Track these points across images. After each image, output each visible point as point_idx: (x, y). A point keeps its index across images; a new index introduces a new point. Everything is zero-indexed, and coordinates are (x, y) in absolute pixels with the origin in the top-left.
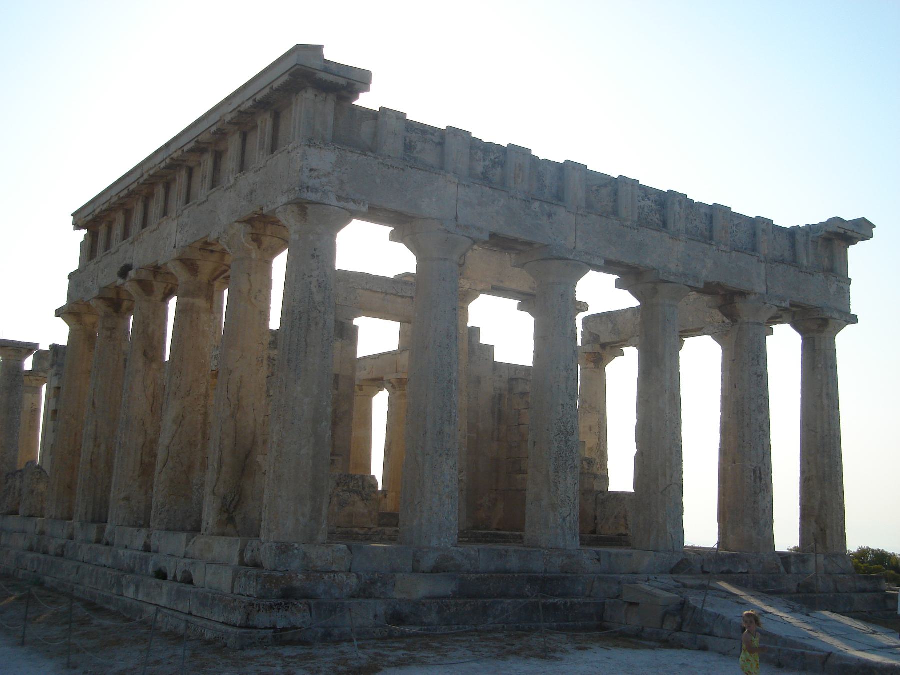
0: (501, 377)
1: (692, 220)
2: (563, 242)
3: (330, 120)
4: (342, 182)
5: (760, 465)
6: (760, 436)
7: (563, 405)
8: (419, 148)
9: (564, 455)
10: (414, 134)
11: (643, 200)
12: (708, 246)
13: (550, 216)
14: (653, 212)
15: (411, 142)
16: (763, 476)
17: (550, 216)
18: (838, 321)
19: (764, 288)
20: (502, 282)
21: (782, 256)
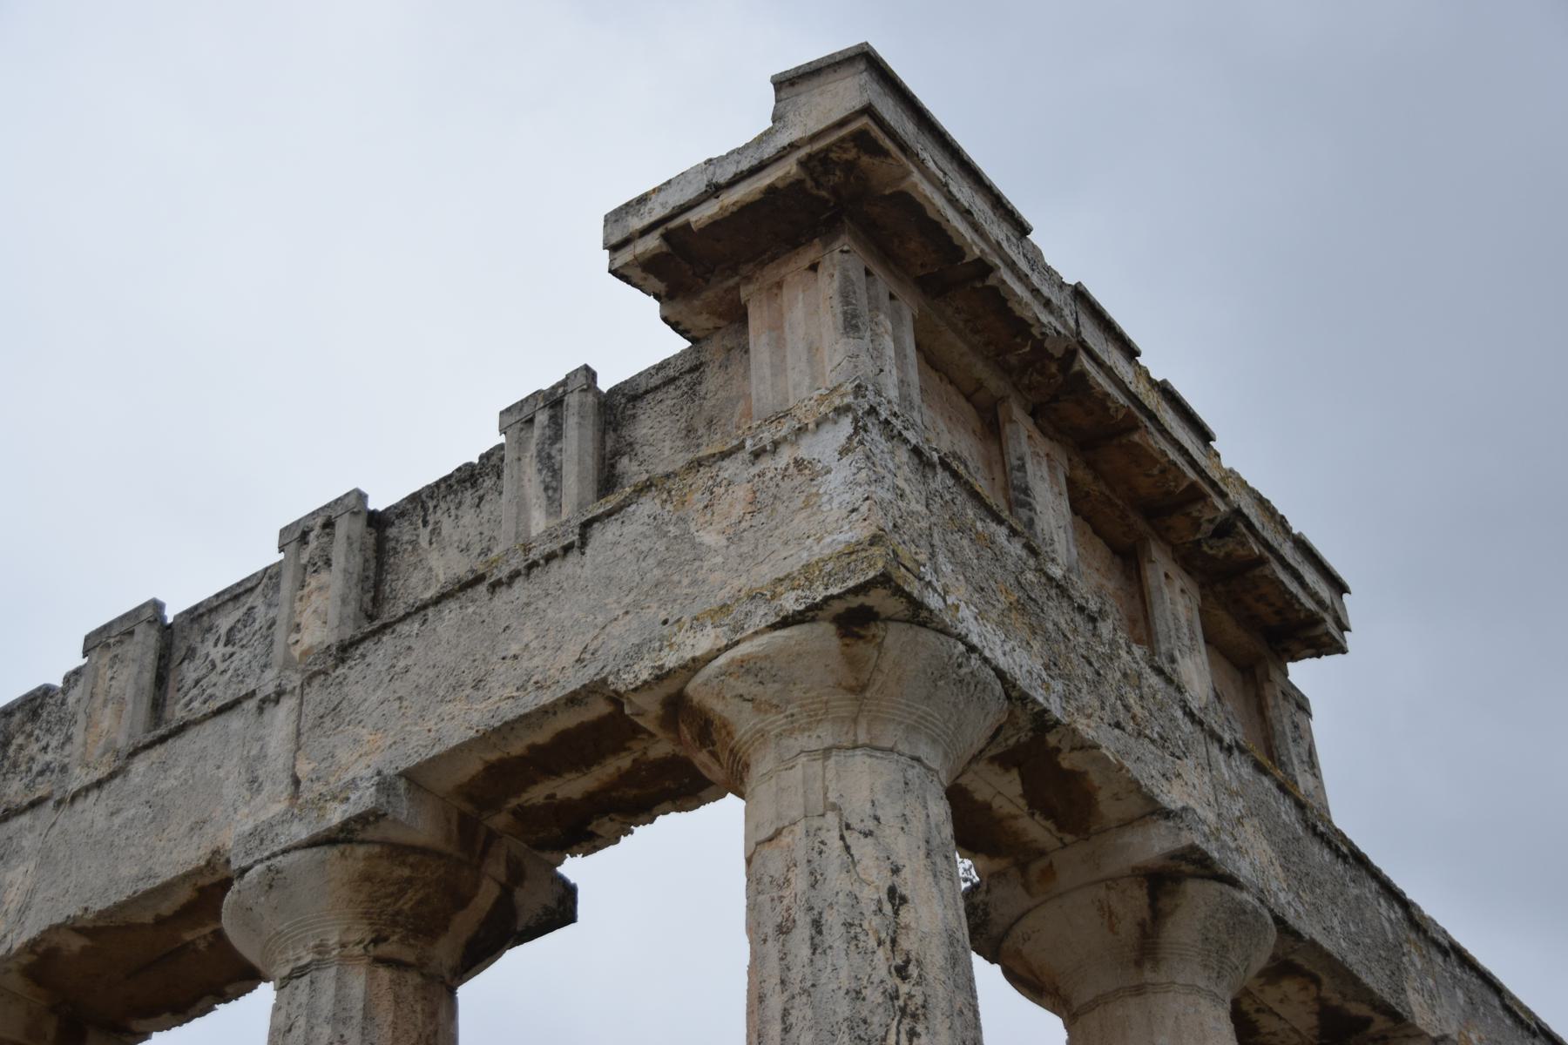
1: (32, 759)
12: (25, 820)
18: (722, 660)
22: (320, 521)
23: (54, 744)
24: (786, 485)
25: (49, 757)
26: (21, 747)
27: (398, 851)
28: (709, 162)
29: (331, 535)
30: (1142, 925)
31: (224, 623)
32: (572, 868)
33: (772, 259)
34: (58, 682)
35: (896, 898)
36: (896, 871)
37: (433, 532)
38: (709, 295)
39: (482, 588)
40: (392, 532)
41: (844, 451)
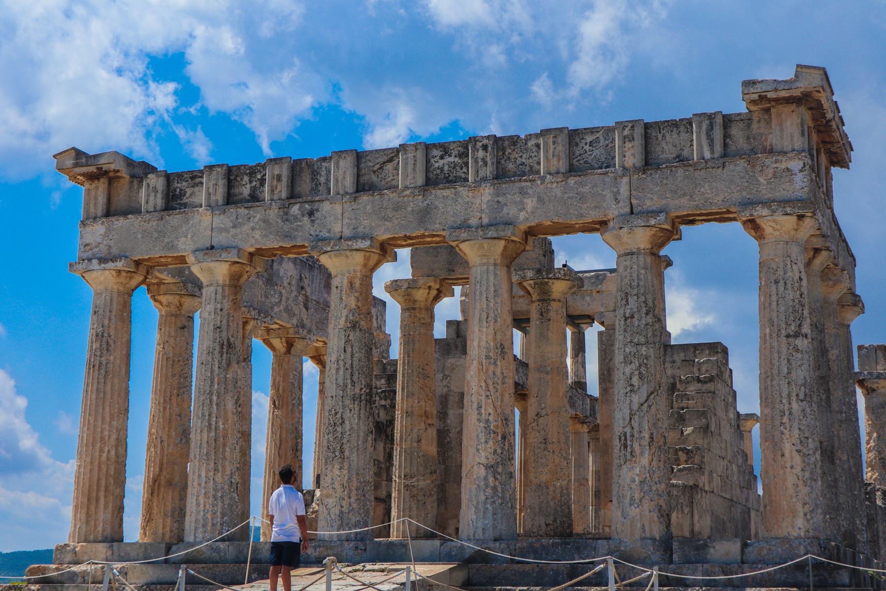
0: (674, 362)
2: (327, 235)
3: (102, 200)
4: (109, 246)
5: (625, 430)
6: (627, 393)
7: (332, 397)
8: (188, 194)
9: (331, 447)
10: (184, 183)
11: (442, 158)
12: (528, 184)
13: (311, 214)
14: (458, 169)
15: (181, 190)
16: (629, 443)
17: (311, 214)
18: (768, 218)
19: (628, 210)
20: (453, 271)
21: (678, 157)
22: (630, 125)
23: (524, 156)
24: (784, 174)
25: (524, 161)
26: (510, 153)
27: (662, 230)
28: (775, 80)
29: (633, 130)
30: (810, 259)
31: (589, 138)
32: (683, 227)
33: (781, 104)
34: (523, 137)
35: (801, 279)
36: (800, 272)
37: (663, 136)
38: (760, 106)
39: (690, 168)
40: (649, 131)
41: (801, 171)
